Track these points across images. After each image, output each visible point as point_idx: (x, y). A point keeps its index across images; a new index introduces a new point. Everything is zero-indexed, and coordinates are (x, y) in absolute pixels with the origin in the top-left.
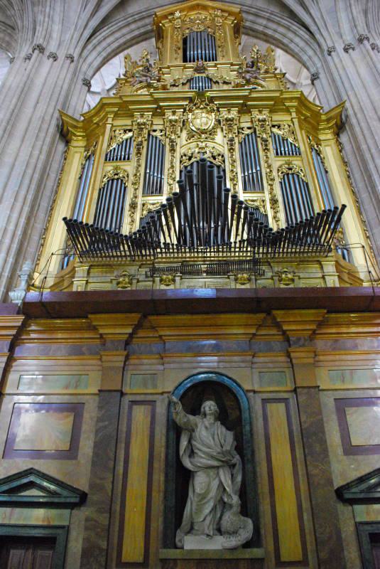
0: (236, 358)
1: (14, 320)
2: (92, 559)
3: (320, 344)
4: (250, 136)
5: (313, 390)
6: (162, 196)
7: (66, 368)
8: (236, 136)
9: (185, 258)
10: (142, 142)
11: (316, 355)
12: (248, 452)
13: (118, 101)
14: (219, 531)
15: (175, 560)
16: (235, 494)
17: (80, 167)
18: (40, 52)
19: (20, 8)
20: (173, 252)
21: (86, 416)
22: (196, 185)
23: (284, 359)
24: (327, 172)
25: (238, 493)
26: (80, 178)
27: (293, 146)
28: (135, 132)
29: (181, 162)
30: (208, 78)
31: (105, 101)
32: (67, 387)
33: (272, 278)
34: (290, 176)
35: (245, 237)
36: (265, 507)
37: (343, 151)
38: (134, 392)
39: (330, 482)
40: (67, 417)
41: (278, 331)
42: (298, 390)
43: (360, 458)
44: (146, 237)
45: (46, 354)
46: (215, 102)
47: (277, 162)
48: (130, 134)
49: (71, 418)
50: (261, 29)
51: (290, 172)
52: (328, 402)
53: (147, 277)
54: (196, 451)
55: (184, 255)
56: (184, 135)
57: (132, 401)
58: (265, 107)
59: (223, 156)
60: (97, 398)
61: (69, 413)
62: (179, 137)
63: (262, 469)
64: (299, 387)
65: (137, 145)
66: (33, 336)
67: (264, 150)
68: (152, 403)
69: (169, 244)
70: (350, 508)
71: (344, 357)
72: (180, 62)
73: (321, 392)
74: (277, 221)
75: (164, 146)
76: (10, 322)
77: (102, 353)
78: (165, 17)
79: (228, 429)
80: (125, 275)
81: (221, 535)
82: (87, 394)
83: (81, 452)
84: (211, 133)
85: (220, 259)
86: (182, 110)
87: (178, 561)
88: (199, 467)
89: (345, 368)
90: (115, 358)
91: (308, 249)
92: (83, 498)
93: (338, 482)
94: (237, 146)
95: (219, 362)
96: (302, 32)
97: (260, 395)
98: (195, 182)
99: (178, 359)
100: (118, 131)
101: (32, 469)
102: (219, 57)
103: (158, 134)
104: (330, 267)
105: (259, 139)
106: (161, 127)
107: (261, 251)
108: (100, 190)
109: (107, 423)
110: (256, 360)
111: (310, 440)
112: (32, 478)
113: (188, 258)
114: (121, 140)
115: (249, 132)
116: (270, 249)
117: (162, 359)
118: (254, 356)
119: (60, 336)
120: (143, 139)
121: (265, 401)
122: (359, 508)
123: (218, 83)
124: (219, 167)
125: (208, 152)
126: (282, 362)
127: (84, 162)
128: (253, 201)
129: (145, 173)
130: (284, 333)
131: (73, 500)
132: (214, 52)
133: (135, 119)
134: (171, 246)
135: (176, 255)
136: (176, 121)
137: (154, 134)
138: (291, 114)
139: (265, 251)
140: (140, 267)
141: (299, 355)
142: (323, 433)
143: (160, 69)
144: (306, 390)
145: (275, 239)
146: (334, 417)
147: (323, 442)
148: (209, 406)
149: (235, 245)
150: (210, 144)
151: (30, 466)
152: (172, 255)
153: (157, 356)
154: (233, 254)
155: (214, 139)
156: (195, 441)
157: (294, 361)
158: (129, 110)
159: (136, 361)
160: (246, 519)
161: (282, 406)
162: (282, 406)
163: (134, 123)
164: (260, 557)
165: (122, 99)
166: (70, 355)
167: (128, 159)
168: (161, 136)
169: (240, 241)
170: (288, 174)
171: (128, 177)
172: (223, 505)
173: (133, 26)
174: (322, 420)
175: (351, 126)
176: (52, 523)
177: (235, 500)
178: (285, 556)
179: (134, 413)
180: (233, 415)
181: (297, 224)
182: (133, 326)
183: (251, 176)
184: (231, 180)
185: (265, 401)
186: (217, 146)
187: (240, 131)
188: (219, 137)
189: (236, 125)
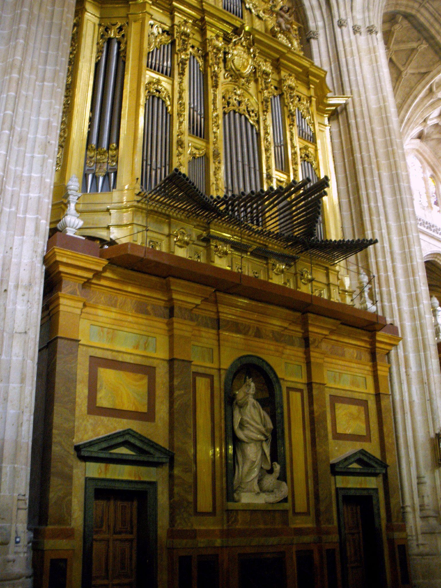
1: (97, 264)
2: (183, 510)
7: (136, 326)
14: (262, 490)
15: (237, 511)
21: (158, 380)
32: (137, 347)
39: (328, 458)
40: (142, 379)
45: (112, 304)
49: (145, 381)
61: (143, 376)
68: (211, 377)
71: (338, 361)
76: (91, 264)
82: (158, 359)
83: (157, 416)
87: (239, 512)
88: (252, 439)
93: (333, 461)
101: (130, 429)
109: (183, 392)
112: (127, 437)
119: (130, 289)
151: (127, 427)
161: (298, 395)
162: (298, 395)
176: (143, 479)
178: (298, 510)
179: (197, 382)
182: (203, 299)
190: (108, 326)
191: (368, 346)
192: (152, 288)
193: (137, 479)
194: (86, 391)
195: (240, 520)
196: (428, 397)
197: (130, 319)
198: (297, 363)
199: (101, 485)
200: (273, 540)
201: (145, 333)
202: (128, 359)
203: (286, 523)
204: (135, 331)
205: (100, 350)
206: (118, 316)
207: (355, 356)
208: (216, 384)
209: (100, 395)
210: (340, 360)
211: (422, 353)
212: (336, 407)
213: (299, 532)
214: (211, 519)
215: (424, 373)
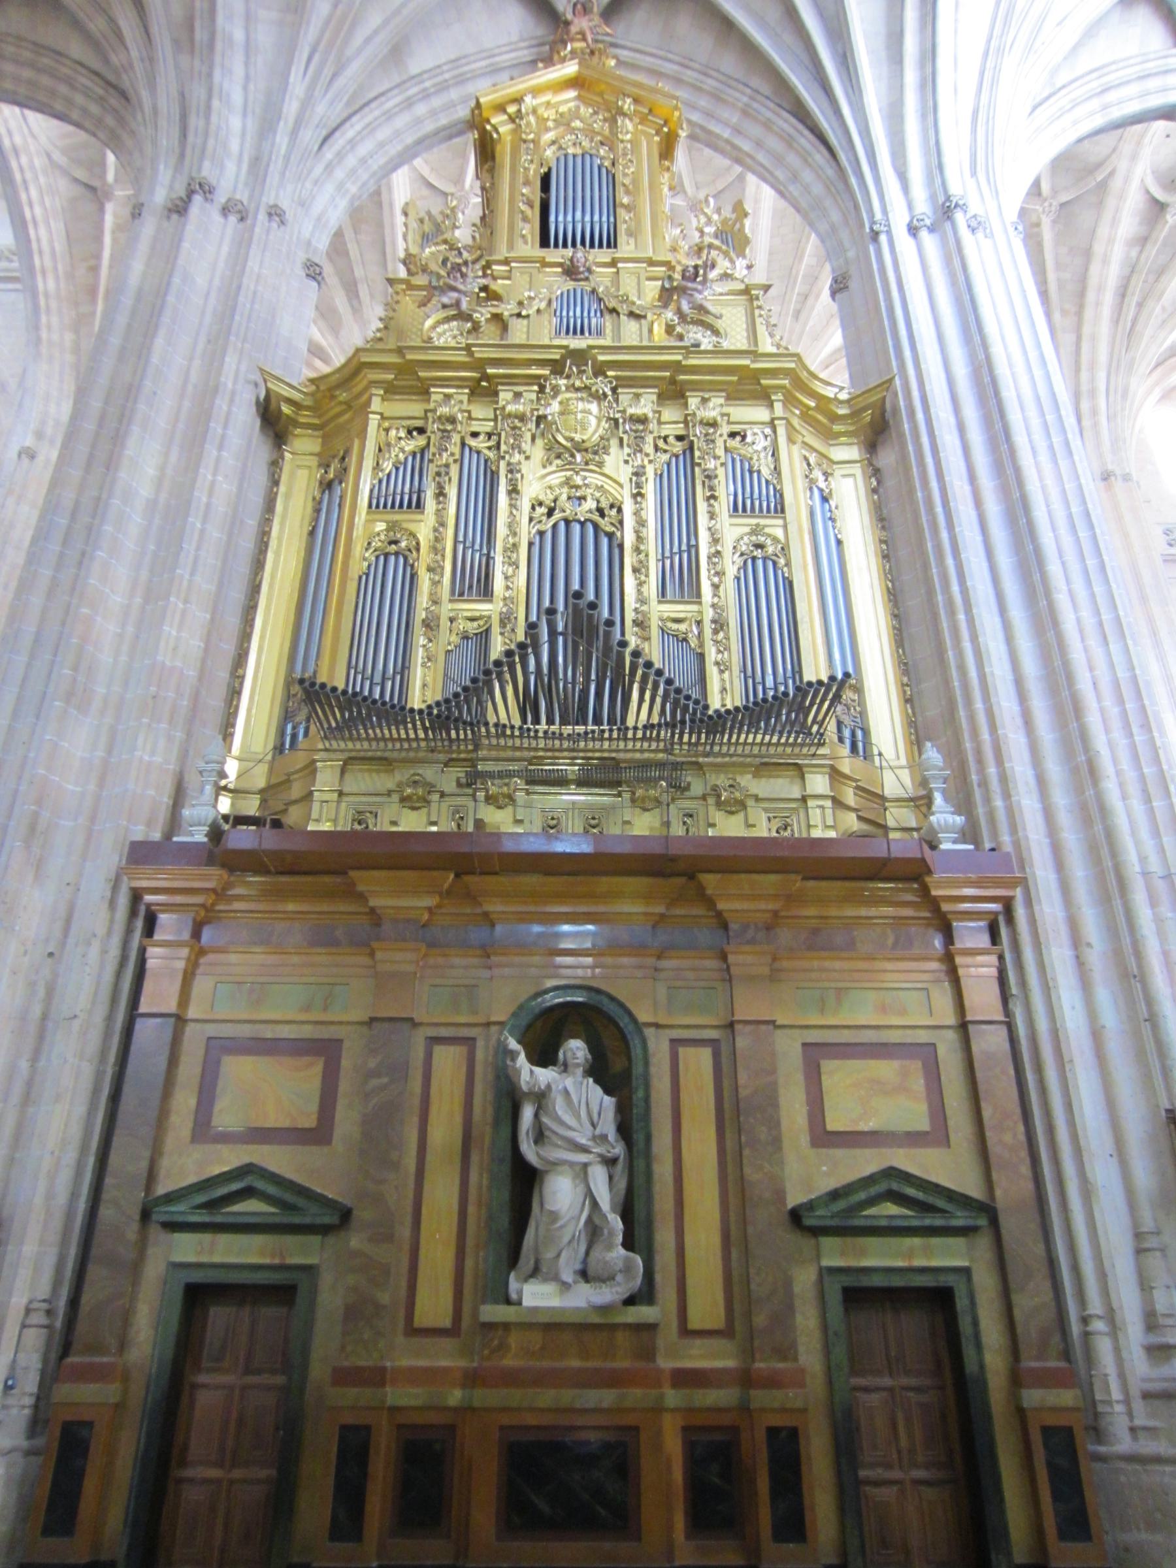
0: (625, 960)
1: (203, 878)
3: (785, 936)
4: (681, 458)
5: (763, 1027)
6: (491, 601)
8: (650, 462)
9: (536, 749)
10: (447, 466)
11: (774, 959)
12: (639, 1137)
13: (393, 359)
14: (584, 1274)
16: (614, 1212)
17: (310, 505)
18: (206, 199)
19: (145, 54)
20: (512, 736)
21: (345, 1063)
22: (561, 634)
23: (713, 964)
24: (839, 542)
25: (619, 1209)
26: (312, 533)
27: (771, 488)
28: (433, 437)
29: (531, 520)
30: (594, 291)
31: (366, 358)
32: (307, 1008)
33: (704, 797)
34: (760, 563)
35: (655, 719)
36: (664, 1237)
37: (881, 490)
38: (435, 1020)
39: (780, 1195)
41: (709, 910)
42: (738, 1027)
43: (839, 1153)
44: (461, 713)
46: (610, 373)
47: (733, 531)
48: (421, 441)
49: (318, 1068)
50: (726, 134)
51: (758, 553)
52: (789, 1048)
53: (459, 785)
54: (547, 1133)
55: (534, 743)
56: (538, 452)
57: (431, 1038)
58: (714, 387)
59: (620, 510)
60: (365, 1030)
62: (527, 458)
63: (663, 1170)
64: (739, 1022)
65: (438, 474)
66: (237, 905)
67: (708, 499)
68: (470, 1042)
69: (504, 726)
70: (813, 1241)
72: (530, 248)
73: (779, 1032)
74: (722, 672)
75: (494, 475)
76: (193, 880)
77: (375, 944)
78: (501, 108)
79: (608, 1091)
80: (415, 782)
81: (587, 1281)
82: (348, 1023)
83: (338, 1133)
84: (594, 453)
85: (606, 755)
86: (536, 388)
89: (826, 984)
90: (399, 956)
91: (779, 740)
92: (345, 1216)
93: (795, 1198)
94: (650, 489)
95: (593, 967)
96: (820, 156)
97: (667, 1031)
98: (560, 628)
99: (517, 959)
100: (393, 433)
102: (622, 238)
103: (480, 443)
104: (818, 783)
105: (697, 469)
106: (489, 426)
107: (686, 738)
108: (360, 578)
109: (385, 1080)
110: (665, 963)
111: (752, 1120)
113: (542, 749)
114: (401, 456)
115: (678, 447)
116: (703, 736)
117: (489, 957)
118: (659, 957)
120: (451, 460)
121: (675, 1042)
122: (827, 1242)
123: (618, 314)
124: (610, 536)
125: (589, 498)
126: (710, 970)
127: (317, 495)
128: (677, 621)
129: (456, 542)
130: (719, 914)
131: (326, 1220)
132: (612, 219)
133: (432, 406)
134: (508, 732)
135: (518, 742)
136: (522, 418)
137: (472, 442)
138: (771, 406)
139: (693, 740)
140: (446, 765)
141: (743, 959)
142: (776, 1106)
143: (488, 265)
144: (749, 1028)
145: (717, 723)
146: (799, 1077)
147: (774, 1124)
148: (576, 1049)
149: (635, 734)
150: (594, 479)
151: (246, 1159)
152: (510, 743)
153: (479, 952)
154: (630, 745)
155: (600, 464)
156: (546, 1113)
157: (733, 970)
158: (419, 379)
159: (440, 960)
160: (631, 1254)
161: (706, 1054)
163: (429, 415)
164: (651, 1321)
165: (403, 356)
166: (313, 944)
167: (418, 506)
168: (489, 448)
169: (645, 727)
170: (754, 559)
171: (418, 550)
172: (594, 1230)
173: (421, 109)
174: (775, 1083)
175: (901, 435)
177: (617, 1223)
178: (694, 1323)
180: (617, 1065)
181: (755, 703)
183: (677, 558)
184: (635, 570)
185: (675, 1042)
186: (609, 486)
187: (661, 444)
188: (616, 463)
189: (651, 432)
190: (250, 979)
191: (927, 914)
192: (330, 895)
193: (277, 1261)
194: (193, 1102)
195: (513, 1346)
196: (1143, 1011)
197: (295, 959)
198: (702, 984)
199: (197, 1277)
200: (606, 1397)
201: (326, 980)
202: (286, 1032)
203: (648, 1354)
204: (305, 980)
205: (229, 1025)
206: (272, 959)
207: (890, 941)
208: (480, 1055)
209: (219, 1105)
210: (832, 959)
211: (1117, 903)
212: (823, 1070)
213: (686, 1378)
214: (447, 1343)
215: (1128, 948)
